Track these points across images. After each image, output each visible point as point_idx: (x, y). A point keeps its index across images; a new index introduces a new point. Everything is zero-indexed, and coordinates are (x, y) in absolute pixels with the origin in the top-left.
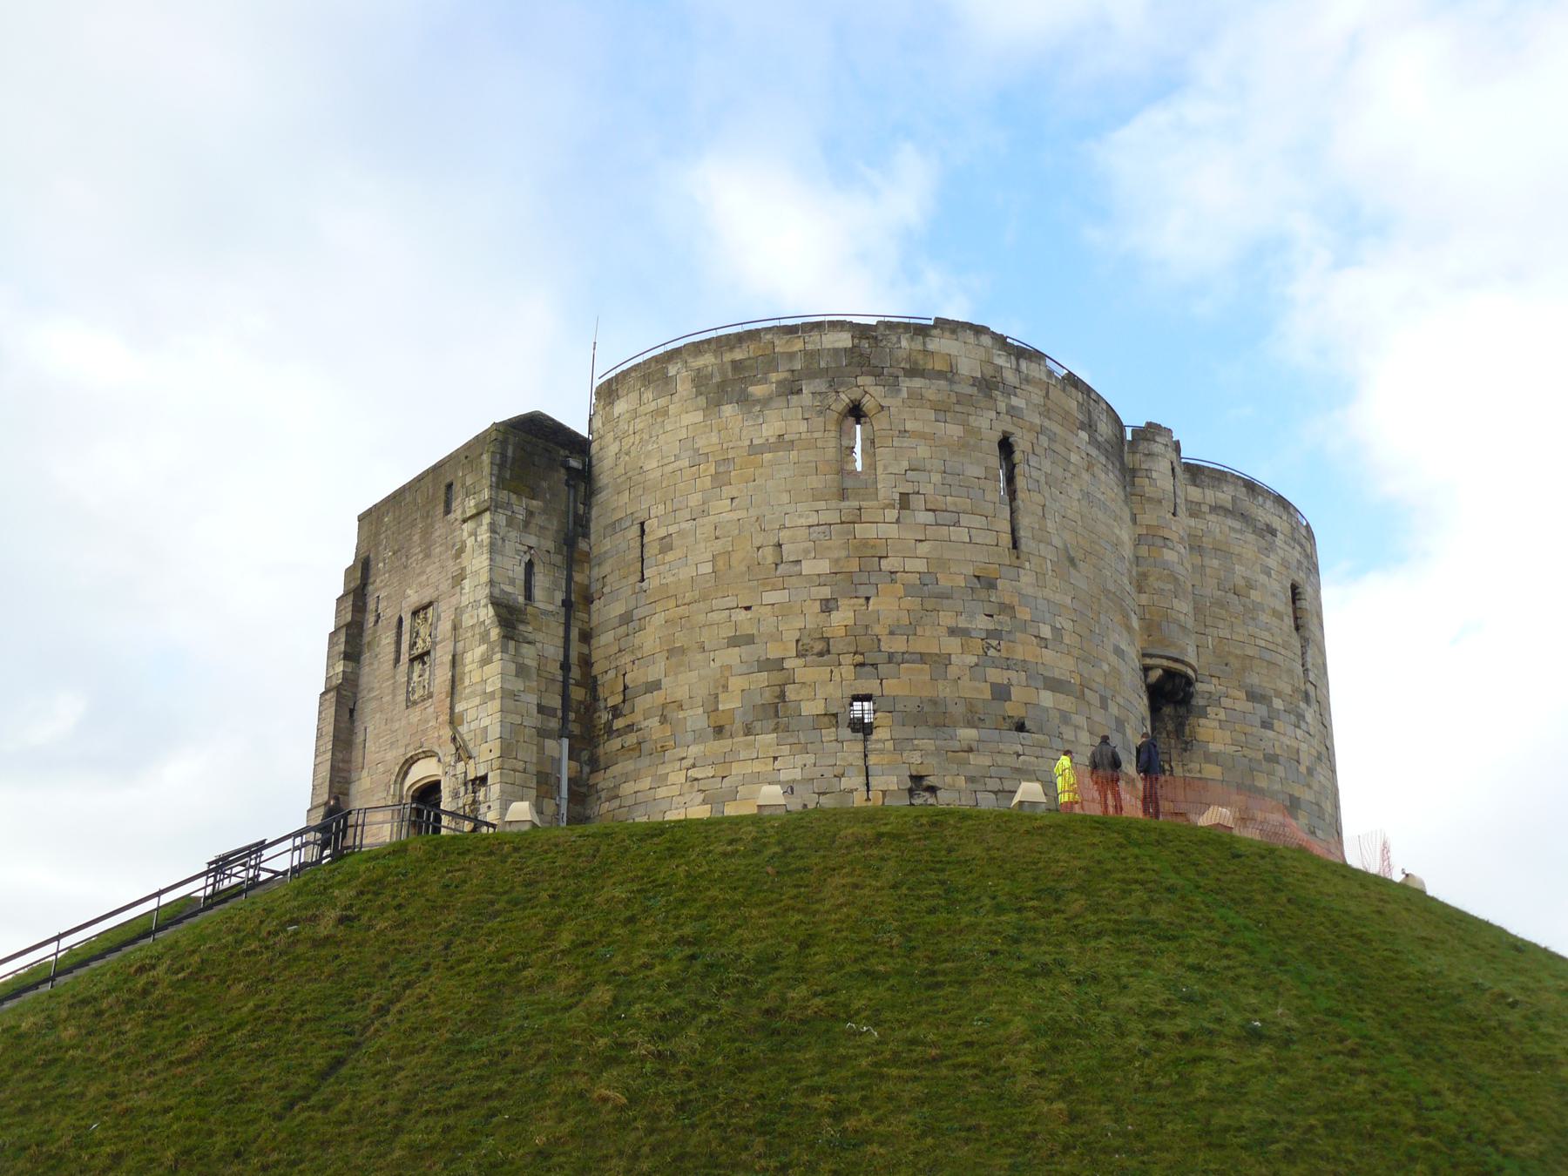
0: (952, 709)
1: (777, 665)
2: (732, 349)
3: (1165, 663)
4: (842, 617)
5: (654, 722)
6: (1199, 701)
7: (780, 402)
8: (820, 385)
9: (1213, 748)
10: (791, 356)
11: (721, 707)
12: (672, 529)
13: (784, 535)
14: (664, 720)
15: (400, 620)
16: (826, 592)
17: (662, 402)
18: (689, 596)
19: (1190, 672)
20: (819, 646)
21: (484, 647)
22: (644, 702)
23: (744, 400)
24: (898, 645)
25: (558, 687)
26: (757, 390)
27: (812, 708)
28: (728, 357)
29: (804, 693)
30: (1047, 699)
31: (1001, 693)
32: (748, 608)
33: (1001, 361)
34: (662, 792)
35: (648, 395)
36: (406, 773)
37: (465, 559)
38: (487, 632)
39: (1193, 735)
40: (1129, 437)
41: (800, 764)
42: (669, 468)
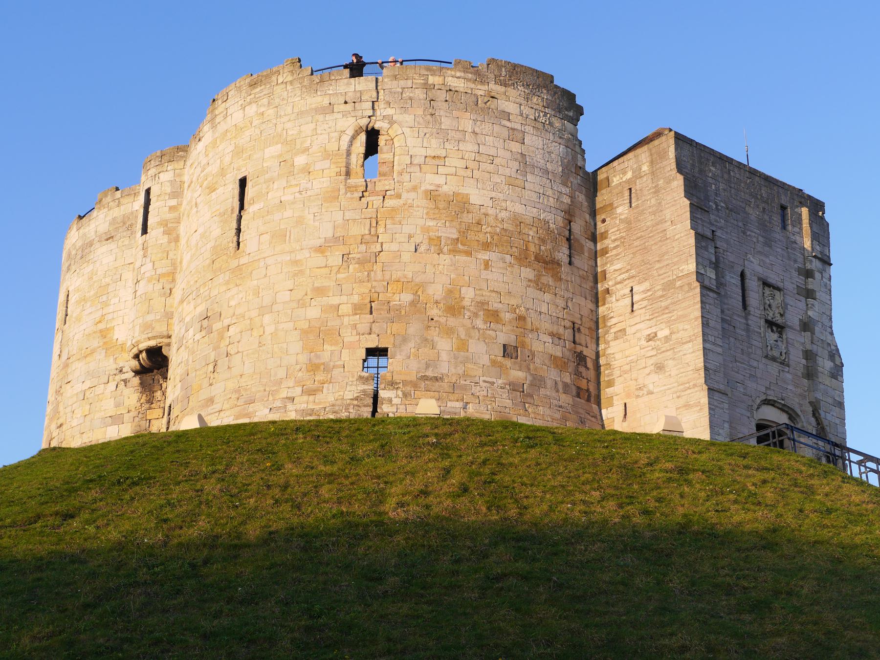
15: (742, 275)
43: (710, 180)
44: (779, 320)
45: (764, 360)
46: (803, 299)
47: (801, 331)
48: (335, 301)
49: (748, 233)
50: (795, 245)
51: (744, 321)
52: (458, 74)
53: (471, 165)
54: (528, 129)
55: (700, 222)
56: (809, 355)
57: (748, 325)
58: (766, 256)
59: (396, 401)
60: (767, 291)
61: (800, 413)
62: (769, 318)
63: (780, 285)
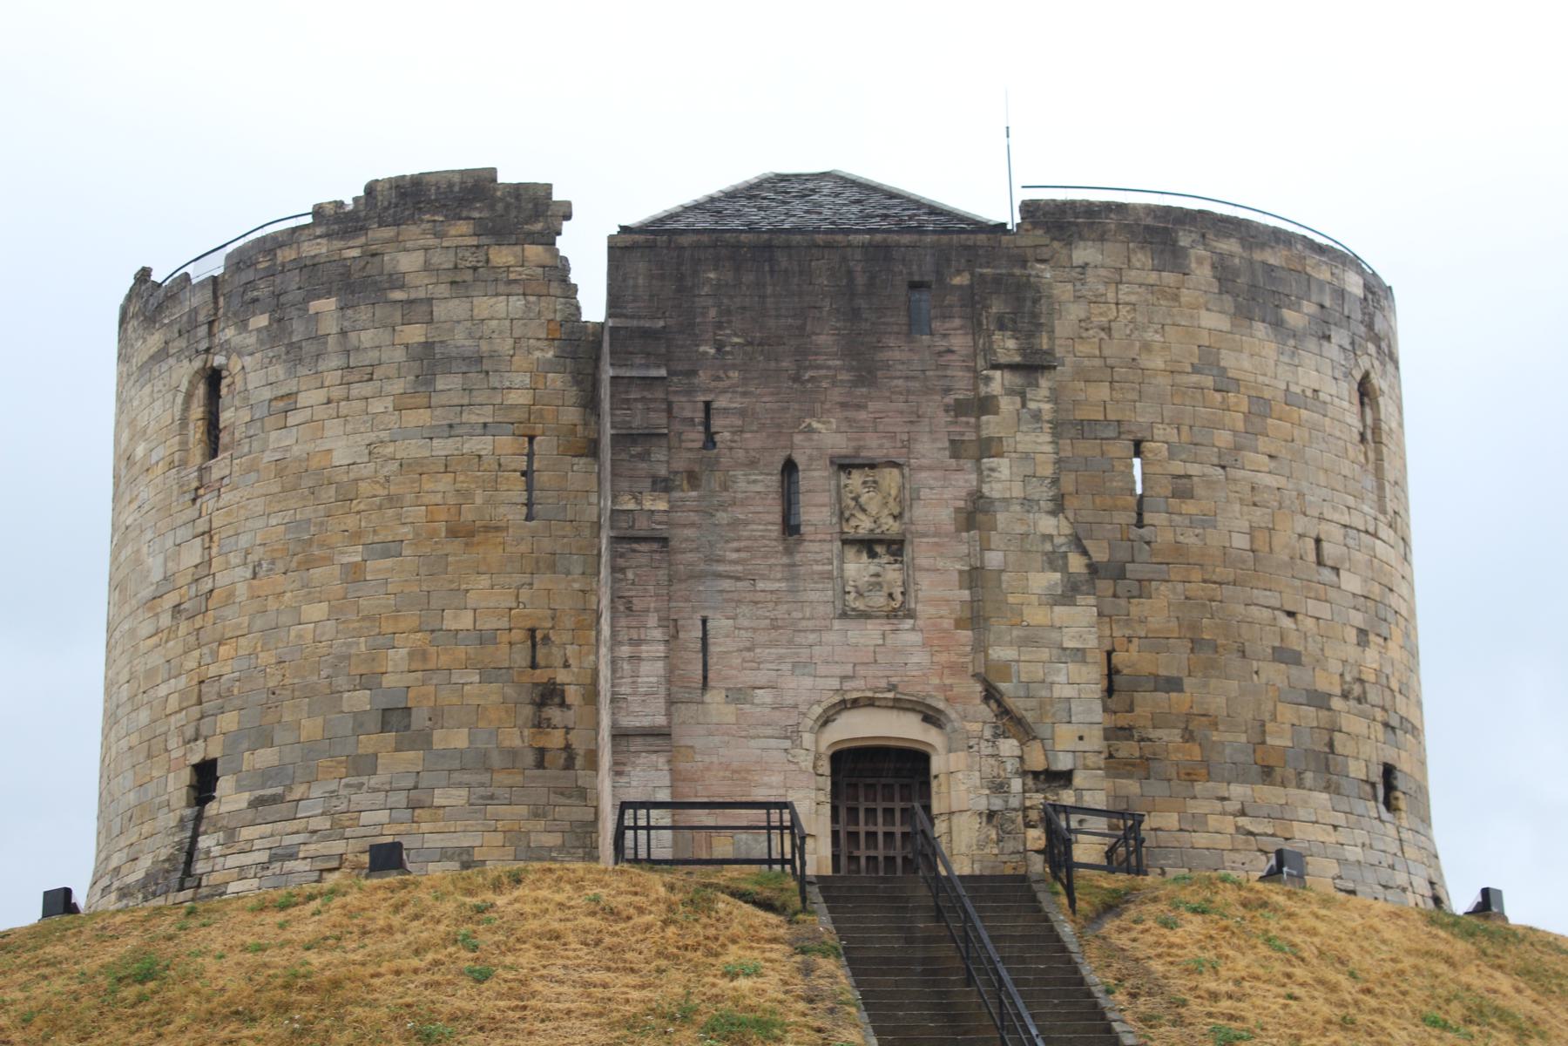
1: (1320, 700)
2: (1262, 246)
4: (1371, 657)
5: (1170, 736)
7: (1312, 344)
10: (1321, 284)
11: (1269, 741)
12: (1194, 469)
13: (1324, 529)
14: (1188, 736)
15: (790, 467)
16: (1358, 619)
17: (1169, 278)
18: (1221, 572)
20: (1357, 689)
21: (1058, 575)
22: (1148, 703)
23: (1278, 324)
27: (1356, 770)
28: (1258, 256)
32: (1291, 614)
34: (1201, 839)
35: (1141, 258)
36: (825, 723)
37: (991, 425)
38: (1065, 556)
41: (1359, 842)
42: (1179, 379)
43: (710, 302)
44: (891, 527)
45: (837, 624)
46: (969, 464)
47: (958, 531)
48: (163, 690)
49: (807, 376)
50: (954, 357)
51: (785, 560)
52: (318, 231)
53: (337, 393)
54: (443, 290)
55: (640, 406)
56: (975, 577)
57: (794, 565)
58: (859, 407)
59: (216, 851)
60: (856, 479)
61: (941, 705)
62: (863, 532)
63: (894, 455)
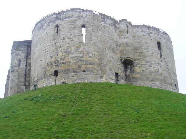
0: (70, 70)
3: (124, 58)
6: (135, 64)
8: (52, 23)
9: (138, 71)
19: (131, 59)
20: (50, 64)
24: (62, 61)
25: (24, 78)
26: (44, 27)
27: (49, 74)
29: (48, 71)
30: (91, 66)
31: (80, 66)
33: (82, 13)
39: (134, 69)
40: (118, 22)
